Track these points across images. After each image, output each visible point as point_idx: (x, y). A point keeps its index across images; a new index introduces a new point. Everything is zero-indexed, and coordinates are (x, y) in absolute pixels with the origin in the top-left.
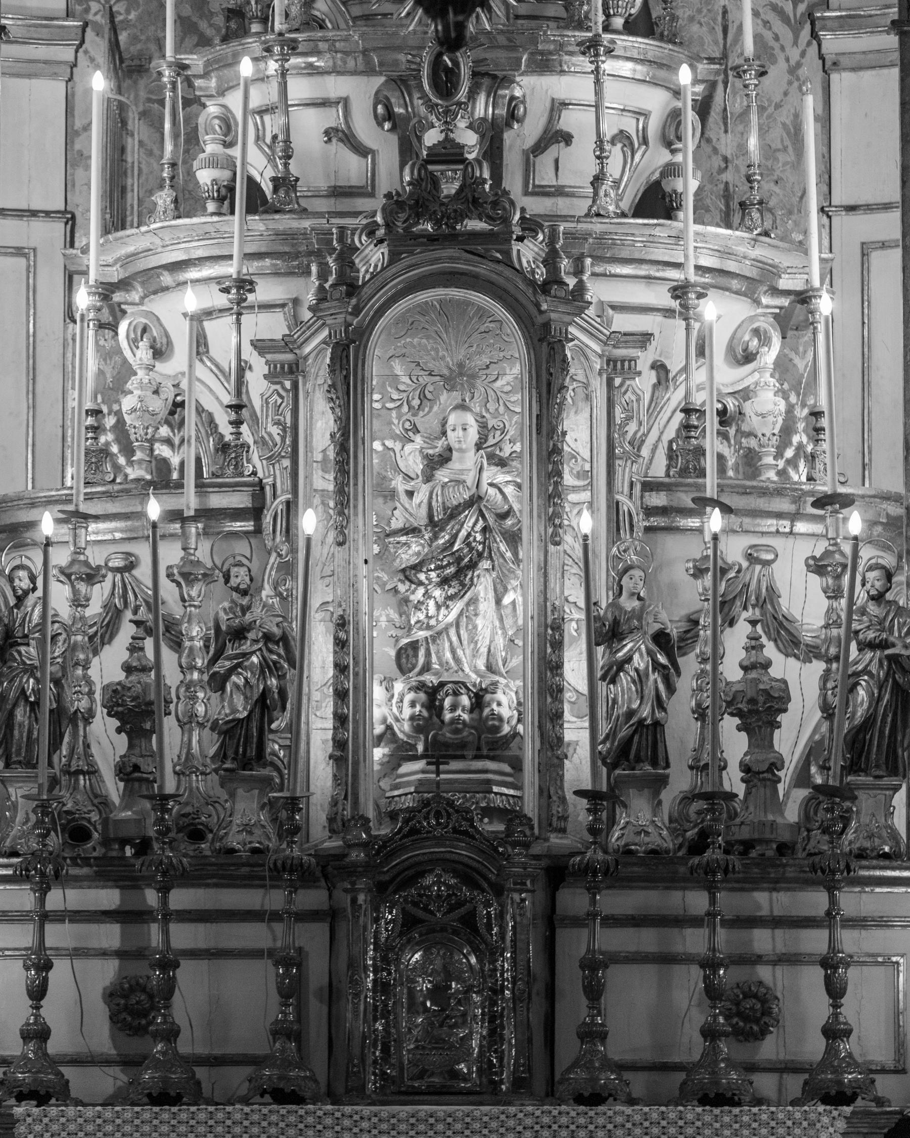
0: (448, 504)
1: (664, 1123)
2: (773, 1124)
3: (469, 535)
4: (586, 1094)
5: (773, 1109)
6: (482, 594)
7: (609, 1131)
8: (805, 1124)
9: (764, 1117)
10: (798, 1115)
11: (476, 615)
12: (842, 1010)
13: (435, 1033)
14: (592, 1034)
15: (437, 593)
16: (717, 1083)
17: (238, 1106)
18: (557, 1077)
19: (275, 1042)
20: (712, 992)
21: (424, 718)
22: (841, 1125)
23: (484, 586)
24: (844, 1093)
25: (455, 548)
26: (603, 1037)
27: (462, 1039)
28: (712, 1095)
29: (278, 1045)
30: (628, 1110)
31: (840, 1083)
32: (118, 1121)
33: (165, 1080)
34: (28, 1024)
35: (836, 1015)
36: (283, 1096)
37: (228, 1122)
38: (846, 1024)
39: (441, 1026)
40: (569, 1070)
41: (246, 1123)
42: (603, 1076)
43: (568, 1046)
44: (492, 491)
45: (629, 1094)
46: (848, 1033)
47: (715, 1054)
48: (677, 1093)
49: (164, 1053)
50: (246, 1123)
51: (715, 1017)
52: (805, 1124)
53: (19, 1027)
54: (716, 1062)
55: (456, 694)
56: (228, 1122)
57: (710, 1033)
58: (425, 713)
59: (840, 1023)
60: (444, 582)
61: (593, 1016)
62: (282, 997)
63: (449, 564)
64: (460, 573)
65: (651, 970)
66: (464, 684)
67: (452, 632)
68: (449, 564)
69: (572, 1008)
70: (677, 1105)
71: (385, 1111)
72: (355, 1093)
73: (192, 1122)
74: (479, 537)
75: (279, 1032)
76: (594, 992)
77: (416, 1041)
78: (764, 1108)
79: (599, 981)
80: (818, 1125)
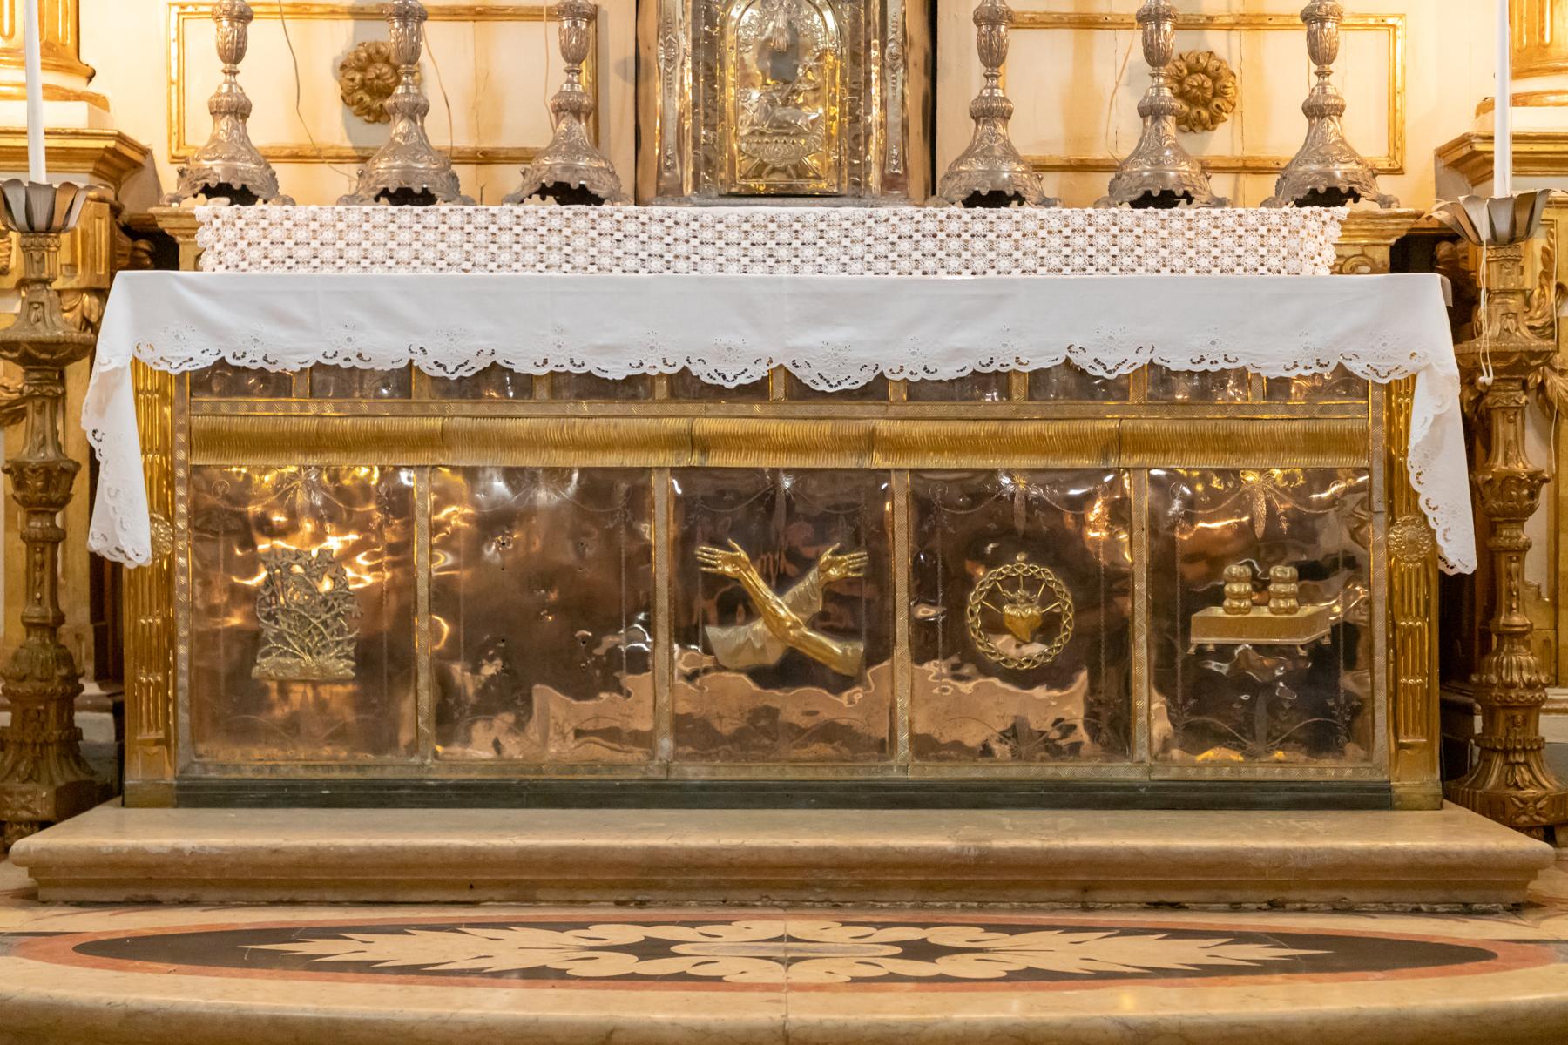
1: (1090, 231)
2: (1240, 231)
4: (984, 192)
5: (1240, 210)
7: (1016, 241)
8: (1285, 231)
9: (1229, 222)
10: (1275, 219)
12: (1331, 79)
13: (778, 114)
14: (990, 113)
16: (1163, 176)
17: (507, 206)
18: (940, 175)
19: (558, 123)
20: (1155, 56)
22: (1334, 232)
24: (1337, 190)
26: (1006, 115)
27: (813, 122)
28: (1156, 193)
29: (563, 126)
30: (1042, 212)
31: (1330, 176)
32: (340, 226)
33: (406, 171)
34: (219, 95)
35: (1323, 86)
36: (567, 194)
37: (493, 228)
38: (1336, 97)
39: (786, 103)
40: (959, 161)
41: (517, 229)
42: (1005, 167)
43: (955, 131)
45: (1042, 193)
46: (1339, 110)
47: (1160, 139)
48: (1107, 194)
49: (406, 137)
50: (517, 229)
51: (1158, 87)
52: (1285, 231)
53: (207, 99)
54: (1160, 150)
56: (493, 228)
57: (1151, 112)
59: (1329, 96)
61: (992, 88)
62: (568, 60)
65: (1065, 36)
69: (962, 78)
70: (1109, 205)
71: (709, 213)
72: (670, 193)
73: (443, 228)
75: (566, 108)
76: (993, 56)
77: (752, 124)
78: (1227, 209)
79: (1001, 39)
80: (1303, 233)
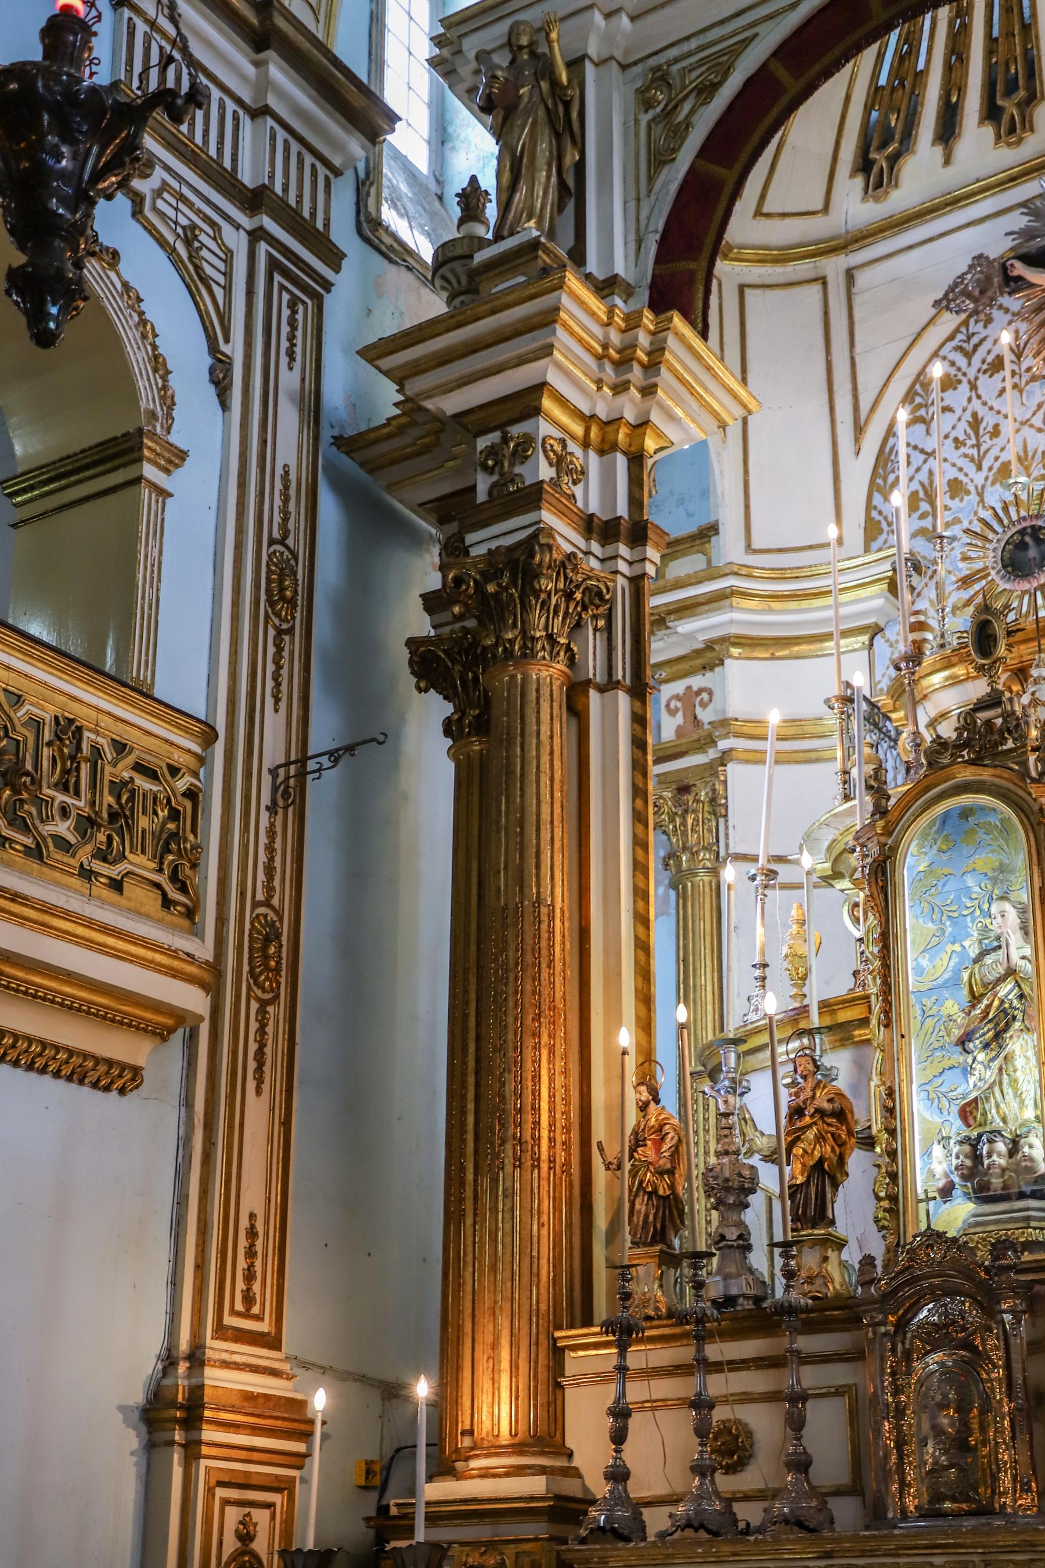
0: (985, 980)
3: (1002, 1002)
6: (1017, 1052)
11: (1015, 1071)
15: (981, 1057)
21: (968, 1168)
23: (1021, 1047)
25: (991, 1016)
44: (1022, 963)
55: (991, 1141)
58: (968, 1163)
60: (986, 1046)
63: (989, 1030)
64: (998, 1036)
66: (999, 1132)
67: (997, 1089)
68: (989, 1030)
74: (1015, 1003)
